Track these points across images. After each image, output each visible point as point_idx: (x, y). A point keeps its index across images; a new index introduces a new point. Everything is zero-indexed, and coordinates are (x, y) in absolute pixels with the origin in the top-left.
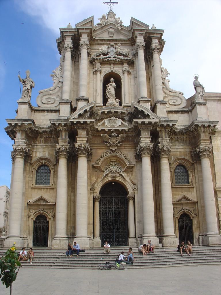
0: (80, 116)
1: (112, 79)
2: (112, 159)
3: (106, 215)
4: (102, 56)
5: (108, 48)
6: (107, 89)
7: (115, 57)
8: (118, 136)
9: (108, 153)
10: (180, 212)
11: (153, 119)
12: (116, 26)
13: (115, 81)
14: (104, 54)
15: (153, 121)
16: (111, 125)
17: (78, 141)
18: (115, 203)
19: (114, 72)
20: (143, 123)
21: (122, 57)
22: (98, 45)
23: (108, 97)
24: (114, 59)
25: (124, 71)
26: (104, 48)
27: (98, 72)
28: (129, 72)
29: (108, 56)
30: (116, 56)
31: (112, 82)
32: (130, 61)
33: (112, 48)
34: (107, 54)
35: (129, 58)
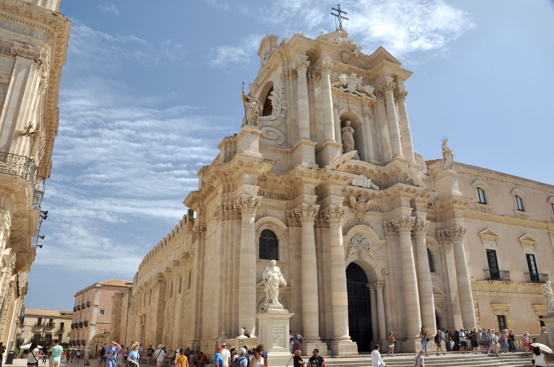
4: (341, 88)
8: (366, 201)
13: (352, 125)
21: (364, 95)
24: (355, 95)
25: (364, 114)
28: (370, 117)
29: (346, 90)
30: (356, 92)
31: (349, 126)
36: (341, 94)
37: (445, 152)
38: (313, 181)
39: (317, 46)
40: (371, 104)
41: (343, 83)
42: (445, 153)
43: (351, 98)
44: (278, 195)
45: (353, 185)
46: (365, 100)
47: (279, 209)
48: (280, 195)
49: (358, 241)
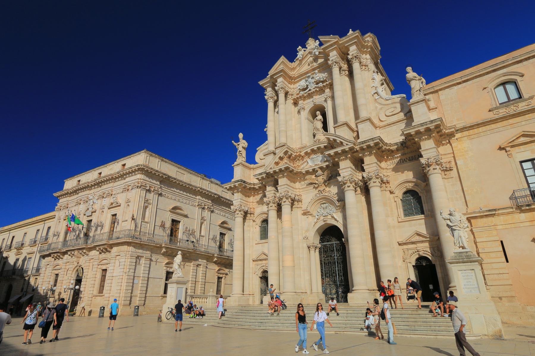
2: (322, 201)
3: (329, 265)
5: (306, 81)
7: (316, 87)
10: (414, 254)
11: (347, 144)
12: (313, 53)
14: (304, 90)
16: (316, 164)
18: (336, 249)
19: (317, 104)
20: (336, 153)
21: (321, 85)
26: (303, 83)
29: (308, 89)
33: (310, 80)
38: (269, 180)
49: (324, 208)
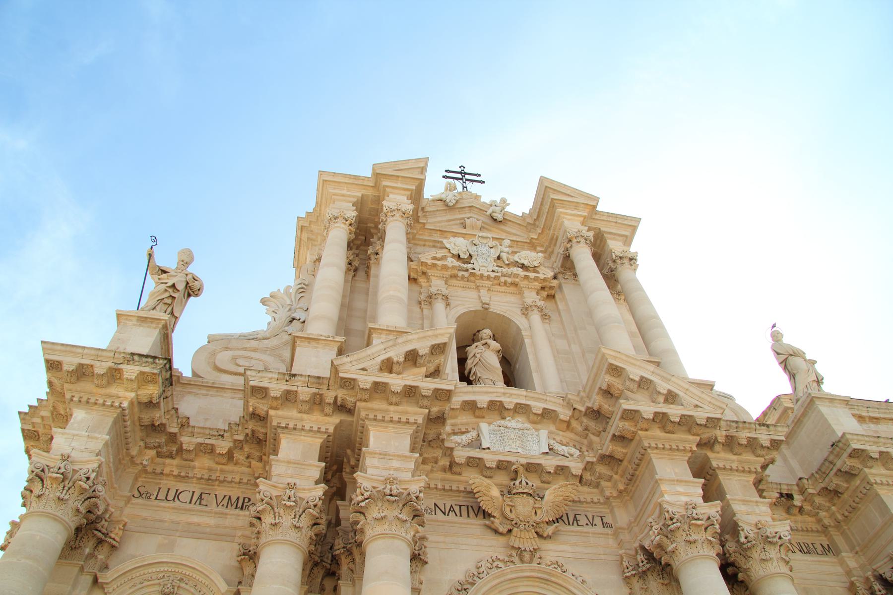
0: (388, 366)
1: (487, 332)
4: (450, 259)
6: (470, 356)
9: (501, 564)
11: (696, 406)
15: (701, 416)
17: (369, 471)
19: (490, 310)
22: (434, 247)
23: (479, 375)
24: (493, 275)
25: (526, 310)
27: (440, 300)
28: (545, 317)
32: (543, 288)
34: (466, 262)
35: (541, 276)
36: (454, 276)
37: (786, 357)
39: (376, 186)
40: (545, 294)
41: (455, 253)
42: (786, 360)
43: (487, 283)
44: (230, 497)
45: (484, 449)
46: (523, 284)
47: (217, 536)
48: (234, 499)
